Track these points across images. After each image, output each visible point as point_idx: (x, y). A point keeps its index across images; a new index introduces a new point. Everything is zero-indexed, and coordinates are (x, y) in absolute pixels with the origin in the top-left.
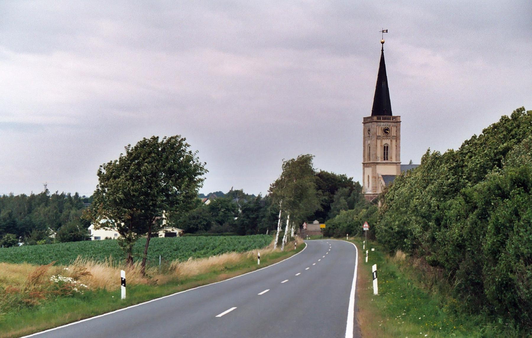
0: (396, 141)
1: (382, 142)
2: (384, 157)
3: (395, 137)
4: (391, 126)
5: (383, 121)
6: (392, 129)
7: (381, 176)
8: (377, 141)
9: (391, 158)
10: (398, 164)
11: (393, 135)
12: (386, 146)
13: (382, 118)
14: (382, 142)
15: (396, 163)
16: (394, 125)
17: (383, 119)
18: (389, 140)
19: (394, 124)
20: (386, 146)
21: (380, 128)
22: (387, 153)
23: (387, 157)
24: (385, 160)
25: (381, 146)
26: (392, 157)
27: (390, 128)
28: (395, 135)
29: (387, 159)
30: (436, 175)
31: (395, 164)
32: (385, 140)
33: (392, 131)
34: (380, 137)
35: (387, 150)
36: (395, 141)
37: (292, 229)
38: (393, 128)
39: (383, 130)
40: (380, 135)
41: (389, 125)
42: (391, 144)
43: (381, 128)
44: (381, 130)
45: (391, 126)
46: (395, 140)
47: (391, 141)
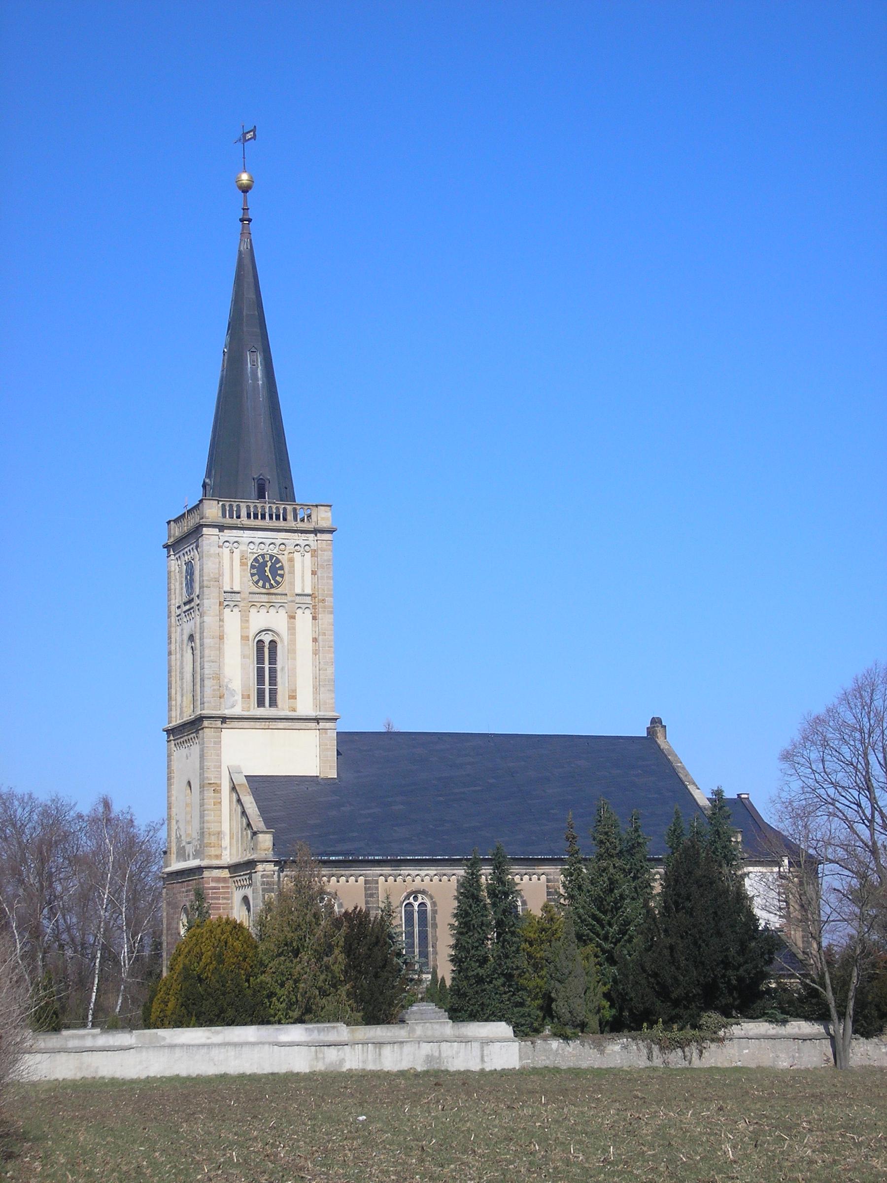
0: (314, 618)
1: (245, 620)
2: (261, 694)
3: (308, 600)
4: (291, 548)
5: (252, 522)
6: (291, 560)
7: (245, 781)
8: (221, 614)
9: (293, 697)
10: (322, 725)
11: (298, 591)
12: (267, 638)
13: (244, 513)
14: (245, 620)
15: (317, 720)
16: (303, 543)
17: (249, 516)
18: (282, 612)
19: (299, 538)
20: (267, 638)
21: (237, 554)
22: (273, 672)
23: (273, 693)
24: (261, 703)
25: (245, 638)
26: (295, 691)
27: (284, 559)
28: (308, 591)
29: (273, 703)
30: (561, 921)
31: (313, 725)
32: (263, 611)
33: (292, 572)
34: (237, 597)
35: (273, 659)
36: (308, 615)
37: (402, 807)
38: (297, 556)
39: (252, 567)
40: (236, 589)
41: (278, 542)
42: (292, 629)
43: (243, 558)
44: (243, 564)
45: (291, 548)
46: (308, 612)
47: (292, 617)
